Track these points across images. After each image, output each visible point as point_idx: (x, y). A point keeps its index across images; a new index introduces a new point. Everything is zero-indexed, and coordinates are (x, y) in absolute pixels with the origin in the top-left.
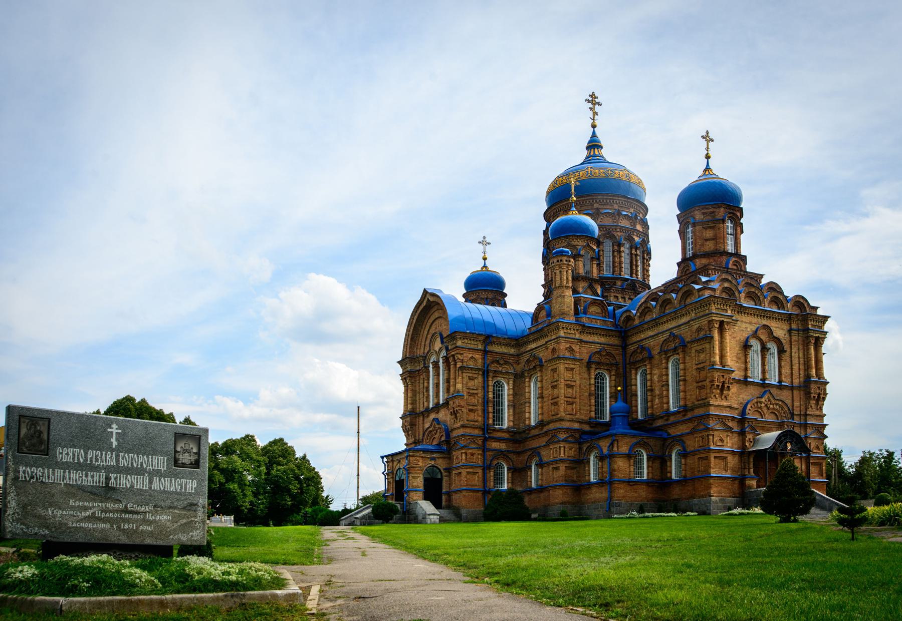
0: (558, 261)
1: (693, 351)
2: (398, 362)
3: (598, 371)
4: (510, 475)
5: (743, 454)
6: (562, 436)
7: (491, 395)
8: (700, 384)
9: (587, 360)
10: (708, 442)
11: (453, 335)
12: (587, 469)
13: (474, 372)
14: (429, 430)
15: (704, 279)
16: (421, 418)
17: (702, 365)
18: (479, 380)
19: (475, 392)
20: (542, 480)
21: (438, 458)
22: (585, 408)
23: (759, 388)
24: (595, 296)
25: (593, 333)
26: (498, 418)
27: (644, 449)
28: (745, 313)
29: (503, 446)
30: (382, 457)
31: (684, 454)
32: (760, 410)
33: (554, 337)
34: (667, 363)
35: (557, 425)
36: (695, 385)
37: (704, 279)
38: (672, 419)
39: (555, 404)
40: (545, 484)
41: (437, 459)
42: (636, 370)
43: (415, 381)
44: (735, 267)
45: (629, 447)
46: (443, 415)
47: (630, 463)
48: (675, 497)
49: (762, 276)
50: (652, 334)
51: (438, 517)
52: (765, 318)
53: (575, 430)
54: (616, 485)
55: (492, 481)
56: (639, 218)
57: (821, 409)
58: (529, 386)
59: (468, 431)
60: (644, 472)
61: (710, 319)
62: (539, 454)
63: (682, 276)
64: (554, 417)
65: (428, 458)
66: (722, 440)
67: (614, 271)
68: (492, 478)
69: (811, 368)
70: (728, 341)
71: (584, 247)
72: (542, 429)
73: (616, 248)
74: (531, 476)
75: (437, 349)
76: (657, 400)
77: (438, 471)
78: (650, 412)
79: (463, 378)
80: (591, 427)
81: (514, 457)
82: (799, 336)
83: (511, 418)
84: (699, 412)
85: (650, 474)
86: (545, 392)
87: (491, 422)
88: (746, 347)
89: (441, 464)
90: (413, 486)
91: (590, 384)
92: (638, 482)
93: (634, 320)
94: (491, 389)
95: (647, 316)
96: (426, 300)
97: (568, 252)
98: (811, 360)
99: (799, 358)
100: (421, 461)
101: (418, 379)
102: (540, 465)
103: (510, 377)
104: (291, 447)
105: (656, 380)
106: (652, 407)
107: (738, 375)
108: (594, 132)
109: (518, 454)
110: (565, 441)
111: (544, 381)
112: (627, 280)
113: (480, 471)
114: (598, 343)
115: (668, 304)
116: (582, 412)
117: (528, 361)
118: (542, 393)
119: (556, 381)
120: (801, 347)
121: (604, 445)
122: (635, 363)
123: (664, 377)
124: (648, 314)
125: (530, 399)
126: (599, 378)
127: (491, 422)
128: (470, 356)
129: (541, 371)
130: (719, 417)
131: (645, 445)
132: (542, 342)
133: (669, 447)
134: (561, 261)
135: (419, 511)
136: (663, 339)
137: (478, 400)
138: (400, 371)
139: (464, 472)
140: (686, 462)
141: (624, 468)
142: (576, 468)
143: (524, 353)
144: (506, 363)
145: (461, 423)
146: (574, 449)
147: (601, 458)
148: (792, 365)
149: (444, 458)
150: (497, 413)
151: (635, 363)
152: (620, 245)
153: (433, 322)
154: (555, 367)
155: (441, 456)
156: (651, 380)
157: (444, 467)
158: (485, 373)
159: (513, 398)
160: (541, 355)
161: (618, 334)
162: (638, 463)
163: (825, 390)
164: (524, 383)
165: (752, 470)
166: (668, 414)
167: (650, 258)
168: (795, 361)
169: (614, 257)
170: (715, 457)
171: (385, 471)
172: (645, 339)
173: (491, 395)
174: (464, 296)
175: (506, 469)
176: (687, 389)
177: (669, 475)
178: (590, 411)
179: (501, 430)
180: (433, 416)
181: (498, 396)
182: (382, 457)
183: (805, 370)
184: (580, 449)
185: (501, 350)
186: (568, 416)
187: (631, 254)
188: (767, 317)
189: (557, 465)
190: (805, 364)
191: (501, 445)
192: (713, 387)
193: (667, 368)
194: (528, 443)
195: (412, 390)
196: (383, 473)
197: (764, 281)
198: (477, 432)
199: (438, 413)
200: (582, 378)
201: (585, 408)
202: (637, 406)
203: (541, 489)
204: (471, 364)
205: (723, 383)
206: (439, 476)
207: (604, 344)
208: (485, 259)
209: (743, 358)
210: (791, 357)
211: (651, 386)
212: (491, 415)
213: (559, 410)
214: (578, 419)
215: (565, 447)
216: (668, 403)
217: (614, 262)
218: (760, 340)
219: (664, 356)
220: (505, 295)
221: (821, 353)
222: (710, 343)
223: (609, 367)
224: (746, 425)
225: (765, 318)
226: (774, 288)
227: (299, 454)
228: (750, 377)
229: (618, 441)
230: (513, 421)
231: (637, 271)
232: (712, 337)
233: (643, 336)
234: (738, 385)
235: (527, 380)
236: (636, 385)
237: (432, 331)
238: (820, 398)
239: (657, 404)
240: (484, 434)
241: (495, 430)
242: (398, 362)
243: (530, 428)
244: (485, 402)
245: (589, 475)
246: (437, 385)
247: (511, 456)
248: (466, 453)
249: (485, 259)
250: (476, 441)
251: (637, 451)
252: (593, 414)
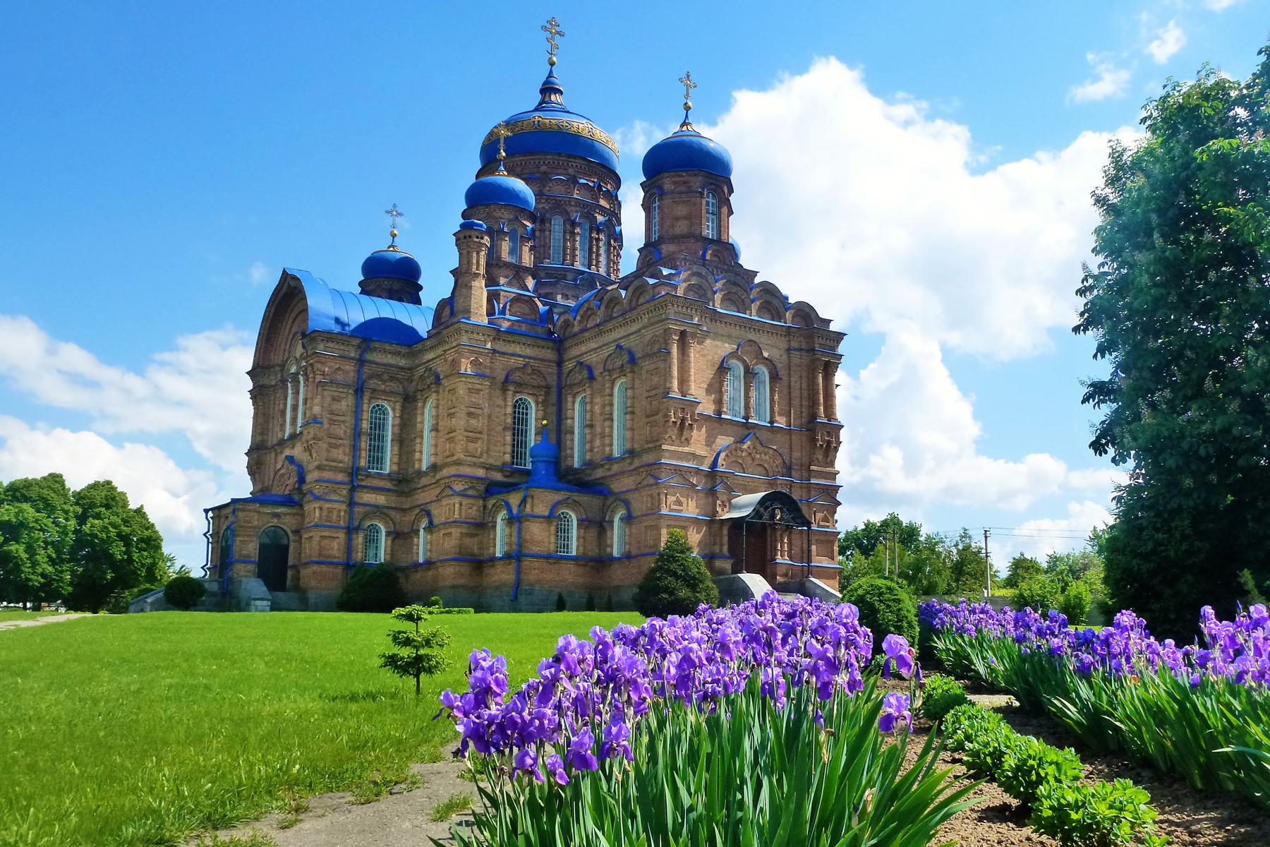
0: (465, 237)
1: (644, 372)
2: (247, 373)
3: (518, 397)
4: (389, 542)
5: (713, 523)
6: (458, 487)
7: (365, 425)
8: (651, 418)
9: (502, 380)
10: (659, 504)
11: (313, 335)
12: (492, 537)
13: (341, 390)
15: (665, 272)
16: (273, 455)
18: (346, 404)
19: (342, 418)
20: (430, 551)
21: (285, 515)
22: (497, 449)
23: (740, 428)
24: (524, 290)
25: (514, 342)
26: (377, 459)
27: (573, 510)
28: (721, 322)
29: (381, 499)
30: (206, 511)
31: (628, 519)
32: (741, 461)
33: (454, 344)
34: (612, 388)
35: (452, 470)
36: (645, 420)
37: (665, 272)
38: (616, 468)
39: (451, 440)
40: (435, 557)
41: (283, 517)
42: (574, 397)
43: (270, 401)
44: (716, 259)
45: (549, 508)
46: (297, 451)
47: (549, 531)
48: (617, 583)
49: (755, 273)
50: (595, 346)
51: (269, 603)
52: (752, 330)
53: (479, 479)
54: (527, 563)
55: (360, 550)
56: (604, 189)
57: (832, 464)
58: (423, 414)
59: (327, 475)
60: (572, 544)
61: (667, 327)
62: (429, 514)
63: (641, 269)
65: (268, 513)
66: (680, 504)
67: (564, 260)
68: (360, 546)
69: (818, 404)
70: (692, 359)
71: (510, 220)
72: (434, 476)
73: (568, 227)
74: (418, 545)
75: (298, 356)
76: (598, 441)
77: (283, 533)
78: (588, 457)
79: (323, 397)
80: (505, 476)
81: (397, 516)
82: (801, 359)
83: (396, 460)
84: (648, 458)
85: (581, 548)
86: (441, 424)
87: (363, 463)
88: (722, 369)
89: (288, 522)
90: (240, 555)
91: (505, 414)
92: (562, 558)
93: (574, 326)
94: (366, 416)
95: (589, 322)
96: (286, 285)
97: (481, 226)
98: (818, 393)
99: (801, 389)
100: (256, 517)
101: (272, 398)
102: (431, 528)
103: (397, 399)
104: (123, 494)
105: (598, 411)
106: (591, 450)
107: (707, 407)
109: (404, 511)
110: (462, 494)
111: (441, 407)
112: (582, 273)
113: (342, 536)
114: (520, 356)
115: (616, 305)
116: (492, 454)
117: (422, 378)
118: (437, 424)
119: (454, 407)
120: (804, 374)
121: (514, 499)
122: (571, 386)
123: (607, 409)
124: (591, 318)
125: (422, 432)
126: (520, 408)
127: (363, 463)
128: (338, 366)
129: (437, 392)
130: (678, 470)
131: (575, 505)
132: (439, 351)
133: (610, 509)
134: (470, 237)
135: (243, 594)
136: (607, 354)
137: (345, 432)
138: (250, 385)
139: (316, 534)
140: (630, 531)
141: (540, 538)
142: (477, 535)
143: (419, 366)
144: (392, 379)
145: (317, 463)
146: (475, 508)
147: (511, 521)
148: (790, 400)
149: (294, 514)
150: (374, 452)
151: (571, 386)
152: (573, 224)
153: (297, 316)
154: (453, 387)
155: (289, 511)
156: (591, 411)
157: (294, 528)
158: (359, 391)
159: (401, 430)
160: (439, 370)
161: (551, 344)
162: (562, 532)
163: (838, 437)
164: (416, 409)
165: (725, 548)
166: (610, 459)
167: (621, 247)
168: (796, 393)
169: (565, 240)
171: (209, 531)
172: (586, 353)
173: (365, 425)
174: (360, 284)
175: (384, 534)
176: (635, 425)
177: (608, 550)
178: (504, 453)
179: (380, 476)
180: (287, 452)
181: (378, 426)
182: (206, 511)
183: (810, 406)
184: (485, 507)
185: (385, 361)
186: (469, 459)
187: (591, 238)
188: (754, 329)
189: (449, 530)
190: (809, 398)
191: (378, 497)
192: (667, 424)
193: (611, 395)
194: (416, 496)
195: (264, 415)
196: (205, 535)
197: (757, 280)
198: (340, 477)
199: (293, 448)
200: (493, 405)
201: (497, 449)
202: (572, 449)
203: (429, 564)
204: (339, 377)
205: (683, 420)
206: (285, 541)
207: (530, 358)
208: (394, 236)
209: (717, 385)
210: (790, 387)
211: (591, 420)
212: (363, 454)
213: (455, 450)
214: (483, 463)
215: (461, 505)
216: (611, 445)
217: (565, 248)
218: (744, 362)
219: (607, 378)
220: (421, 288)
221: (832, 384)
222: (665, 360)
223: (534, 389)
224: (718, 481)
225: (752, 330)
226: (769, 290)
227: (133, 505)
228: (726, 413)
229: (533, 497)
230: (398, 464)
231: (598, 262)
232: (669, 353)
234: (708, 424)
235: (420, 405)
236: (573, 418)
237: (294, 330)
238: (831, 449)
240: (352, 481)
241: (369, 476)
242: (247, 373)
243: (420, 474)
244: (357, 434)
245: (495, 547)
246: (295, 408)
247: (393, 514)
248: (321, 509)
250: (338, 491)
251: (563, 513)
252: (508, 458)
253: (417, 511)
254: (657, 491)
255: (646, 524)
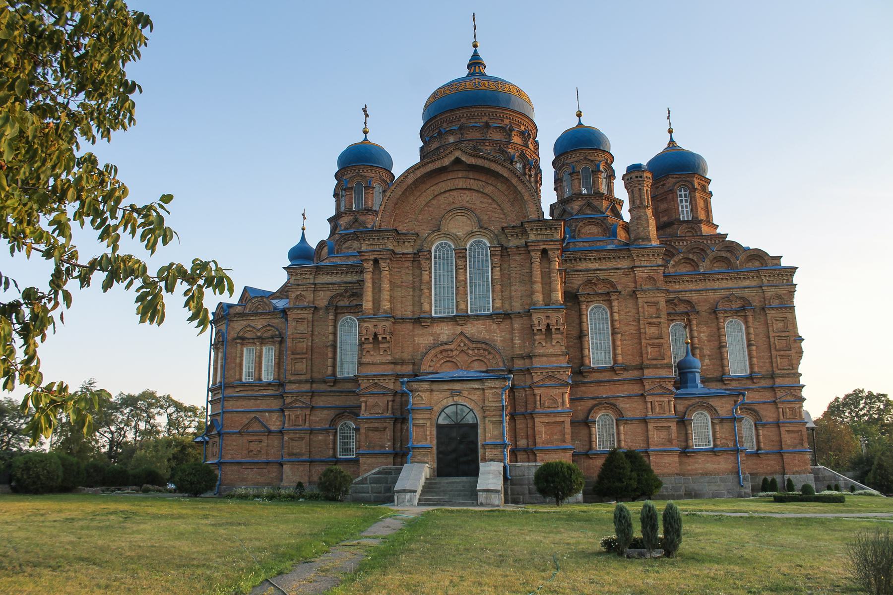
14: (442, 348)
17: (783, 334)
27: (709, 413)
64: (654, 362)
108: (476, 50)
170: (787, 431)
194: (583, 388)
233: (677, 287)
239: (707, 365)
249: (365, 132)
253: (590, 403)
254: (798, 405)
255: (787, 429)
